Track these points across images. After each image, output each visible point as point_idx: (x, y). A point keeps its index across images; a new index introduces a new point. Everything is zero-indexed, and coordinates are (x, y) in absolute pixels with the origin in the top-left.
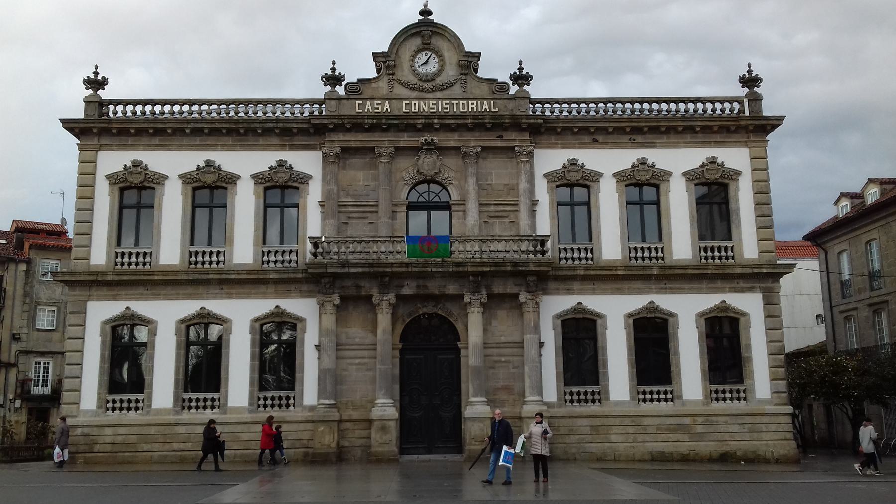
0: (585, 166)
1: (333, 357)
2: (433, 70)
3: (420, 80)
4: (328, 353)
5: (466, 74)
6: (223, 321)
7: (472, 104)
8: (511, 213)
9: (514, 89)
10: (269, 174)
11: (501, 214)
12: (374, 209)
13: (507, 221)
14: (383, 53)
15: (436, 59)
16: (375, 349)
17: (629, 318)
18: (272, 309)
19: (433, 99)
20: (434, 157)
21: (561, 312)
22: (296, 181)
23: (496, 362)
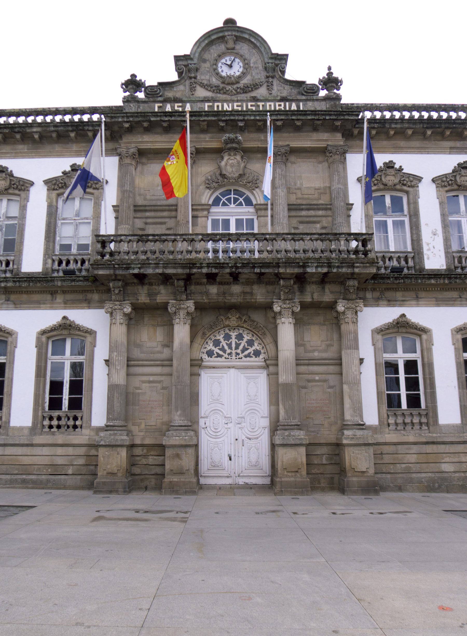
0: (403, 169)
1: (123, 373)
2: (238, 74)
3: (223, 83)
4: (117, 367)
5: (273, 77)
6: (8, 333)
8: (324, 219)
9: (323, 93)
10: (62, 180)
11: (312, 219)
12: (173, 213)
14: (185, 56)
15: (241, 64)
16: (171, 366)
17: (457, 332)
18: (59, 320)
19: (238, 101)
20: (238, 157)
21: (381, 326)
22: (91, 187)
23: (309, 381)
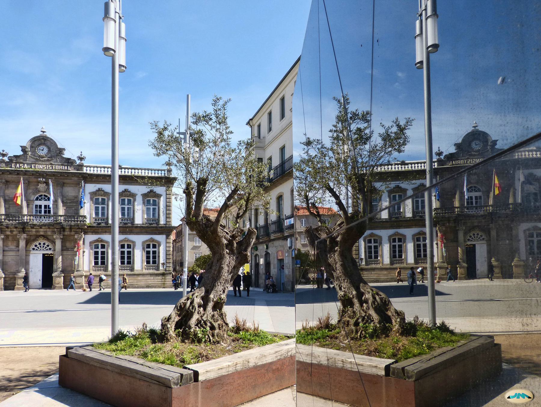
7: (61, 167)
13: (73, 209)
15: (47, 149)
19: (45, 164)
